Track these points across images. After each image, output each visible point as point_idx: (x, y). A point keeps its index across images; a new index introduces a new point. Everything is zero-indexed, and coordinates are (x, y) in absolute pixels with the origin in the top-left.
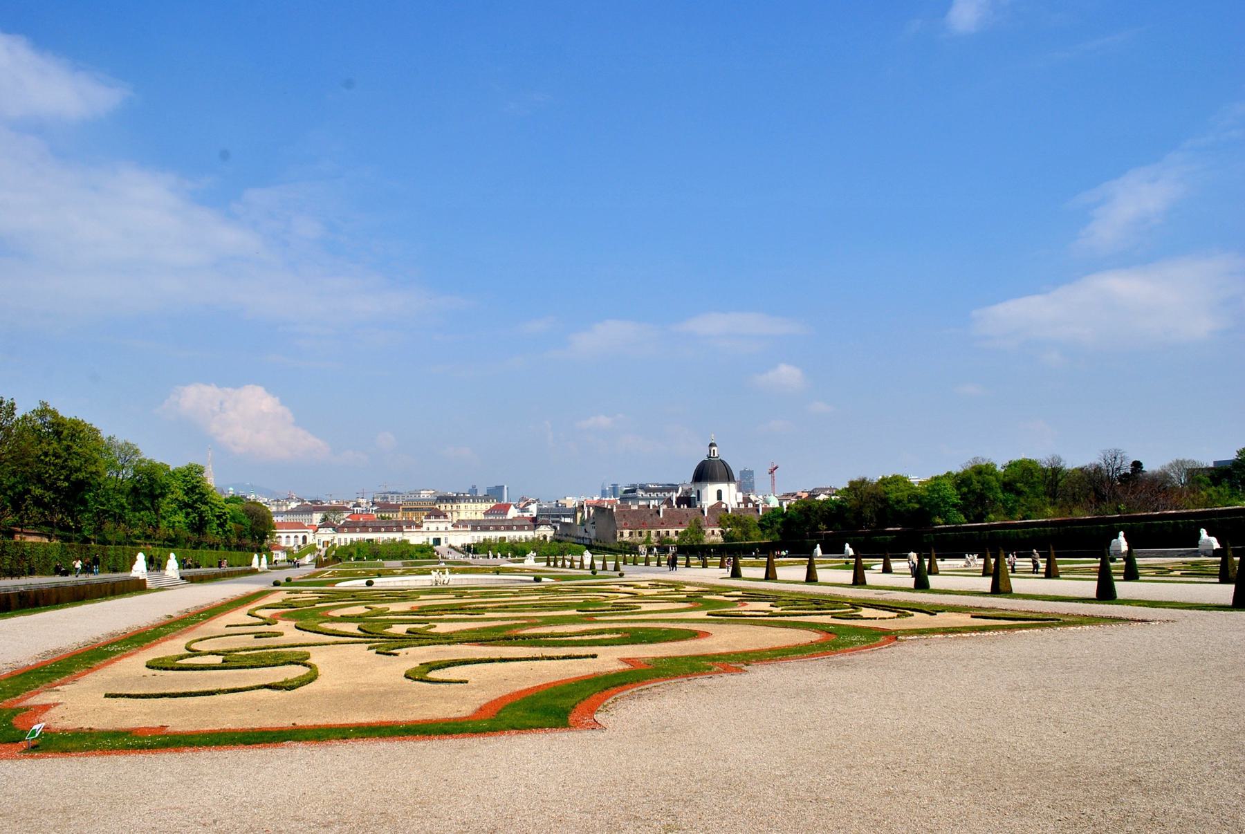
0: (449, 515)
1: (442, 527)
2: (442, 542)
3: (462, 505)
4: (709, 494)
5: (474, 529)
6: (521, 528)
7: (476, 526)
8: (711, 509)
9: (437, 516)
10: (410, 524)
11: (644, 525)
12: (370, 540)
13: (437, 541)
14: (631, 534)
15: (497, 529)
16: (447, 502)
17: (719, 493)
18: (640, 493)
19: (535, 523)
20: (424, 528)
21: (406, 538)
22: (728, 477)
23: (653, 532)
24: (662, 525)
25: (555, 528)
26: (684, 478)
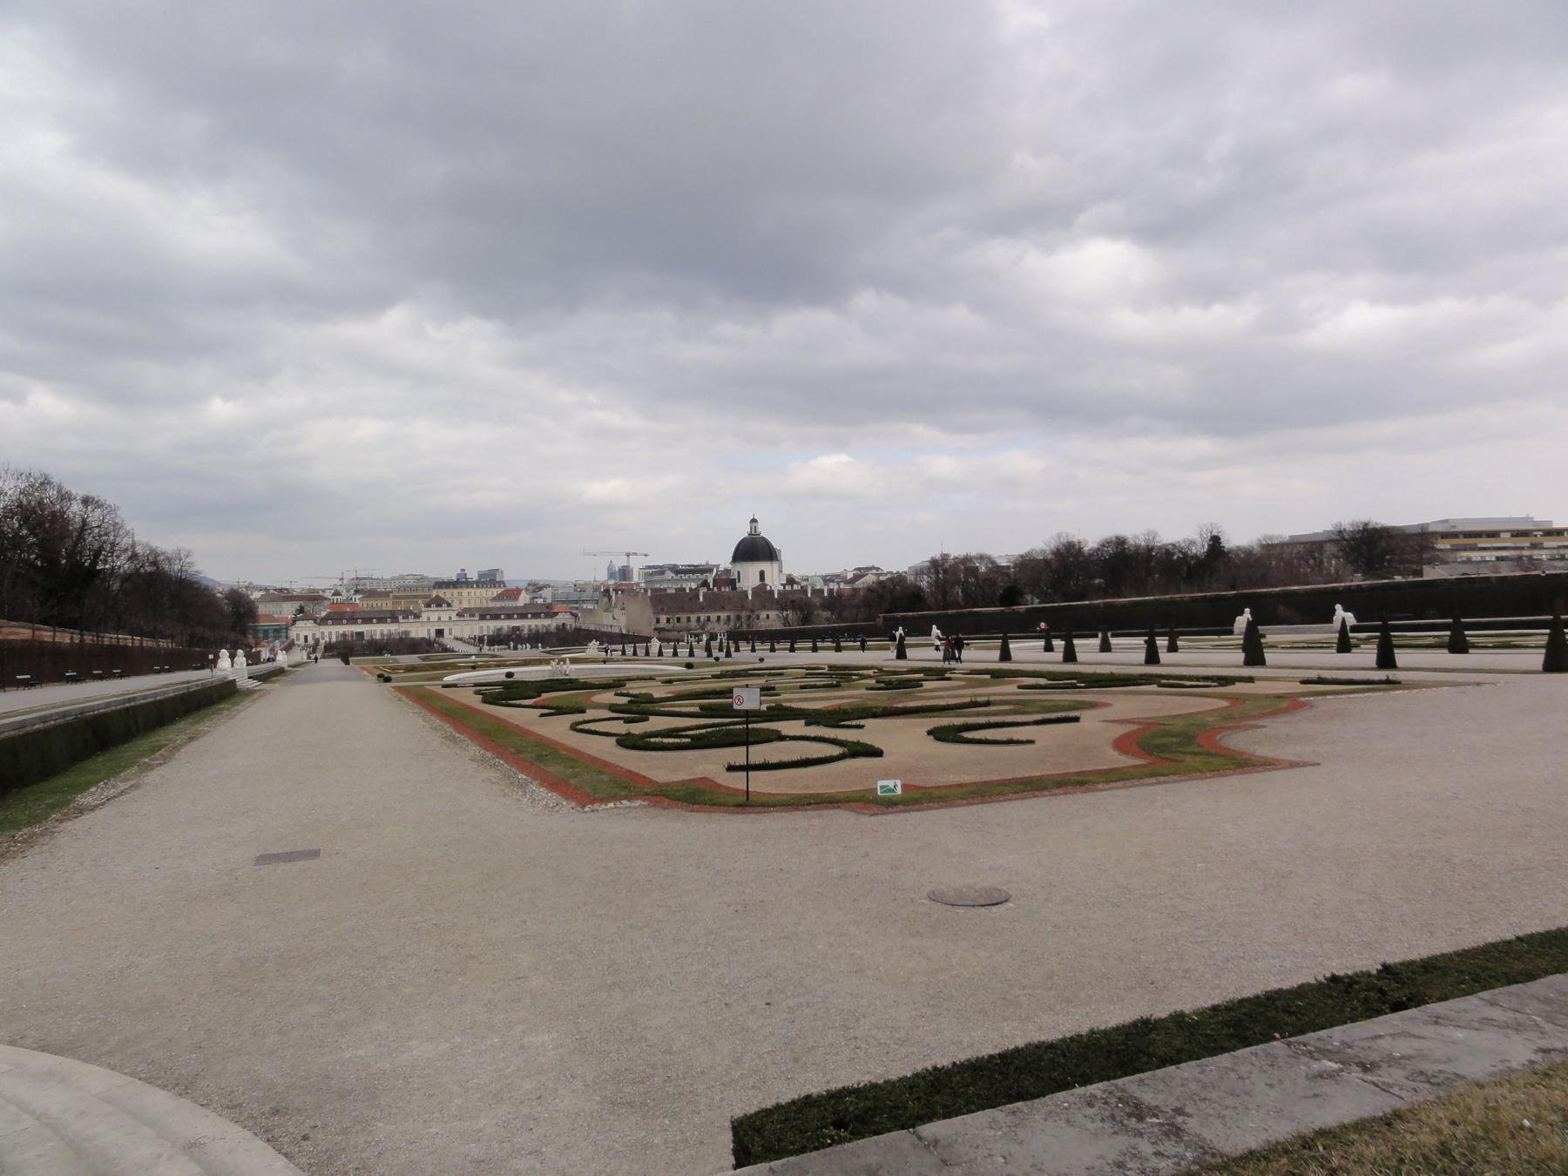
1: (445, 617)
2: (446, 633)
3: (465, 591)
5: (483, 617)
8: (756, 591)
9: (439, 605)
10: (407, 614)
11: (682, 610)
12: (361, 634)
13: (440, 633)
14: (668, 620)
15: (509, 617)
17: (762, 574)
18: (669, 575)
20: (424, 617)
24: (702, 609)
26: (722, 558)
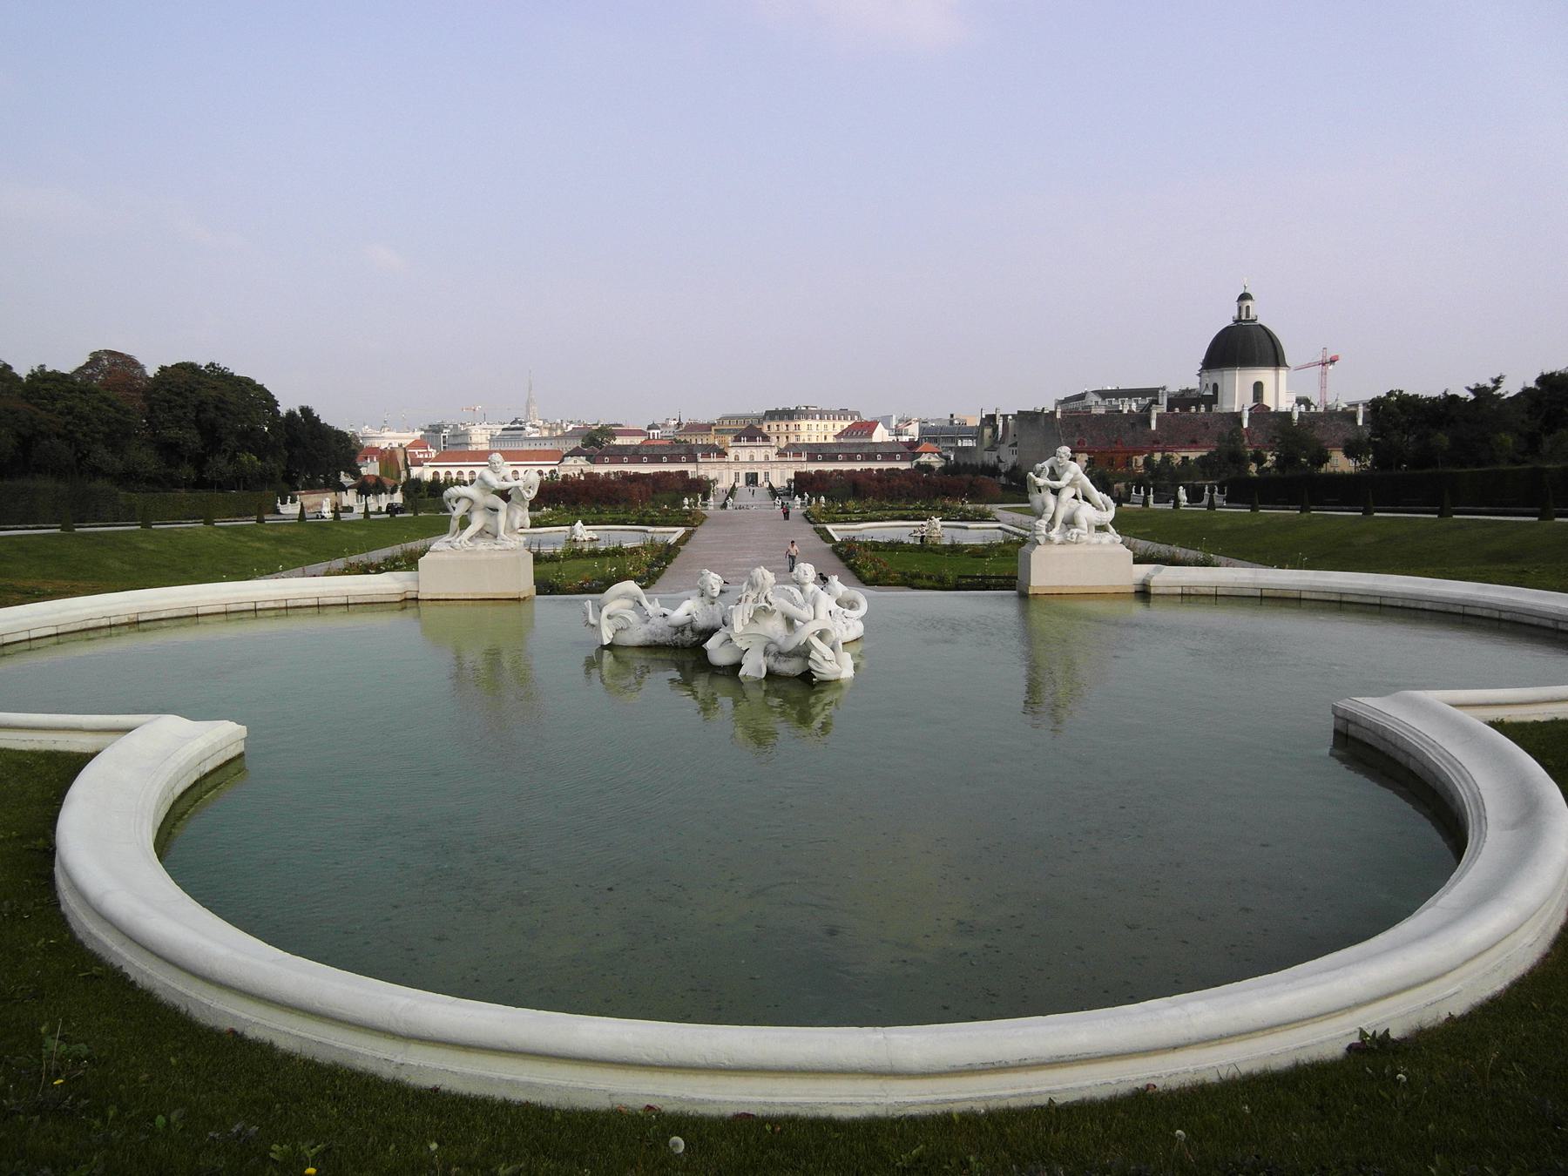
0: (774, 439)
1: (759, 454)
3: (804, 424)
4: (1236, 390)
5: (812, 458)
6: (889, 457)
7: (816, 452)
9: (752, 438)
10: (709, 450)
16: (781, 419)
19: (911, 450)
20: (731, 457)
21: (701, 473)
22: (1275, 358)
23: (1140, 460)
25: (947, 458)
